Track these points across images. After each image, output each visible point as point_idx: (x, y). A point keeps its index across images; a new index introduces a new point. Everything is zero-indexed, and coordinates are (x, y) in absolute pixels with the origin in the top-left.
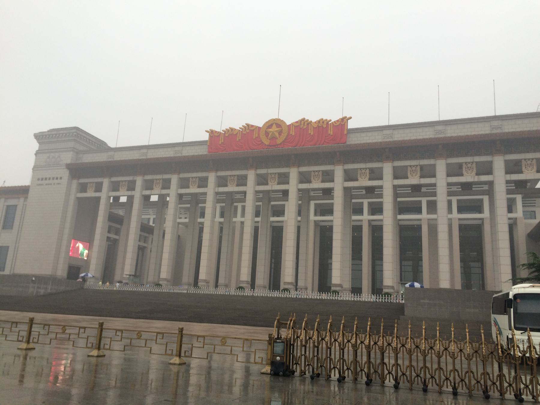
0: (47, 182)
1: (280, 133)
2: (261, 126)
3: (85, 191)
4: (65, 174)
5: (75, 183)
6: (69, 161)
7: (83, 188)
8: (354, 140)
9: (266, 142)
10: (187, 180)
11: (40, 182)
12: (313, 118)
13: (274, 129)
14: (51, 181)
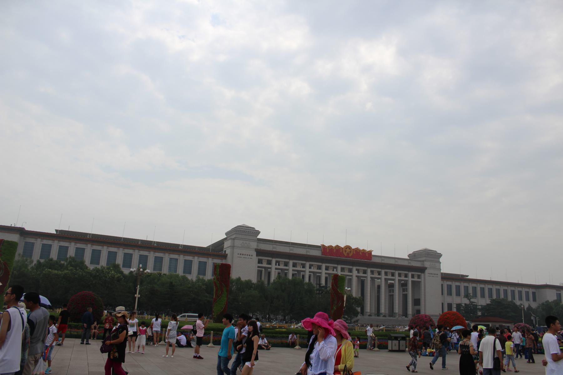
0: (244, 256)
1: (350, 252)
2: (343, 247)
3: (262, 263)
4: (255, 253)
5: (258, 258)
6: (256, 247)
7: (260, 261)
8: (374, 260)
9: (346, 255)
10: (312, 265)
11: (239, 256)
12: (361, 248)
13: (348, 250)
14: (246, 256)
